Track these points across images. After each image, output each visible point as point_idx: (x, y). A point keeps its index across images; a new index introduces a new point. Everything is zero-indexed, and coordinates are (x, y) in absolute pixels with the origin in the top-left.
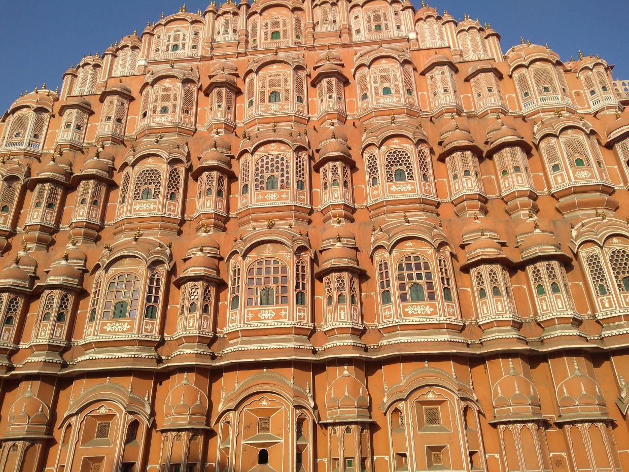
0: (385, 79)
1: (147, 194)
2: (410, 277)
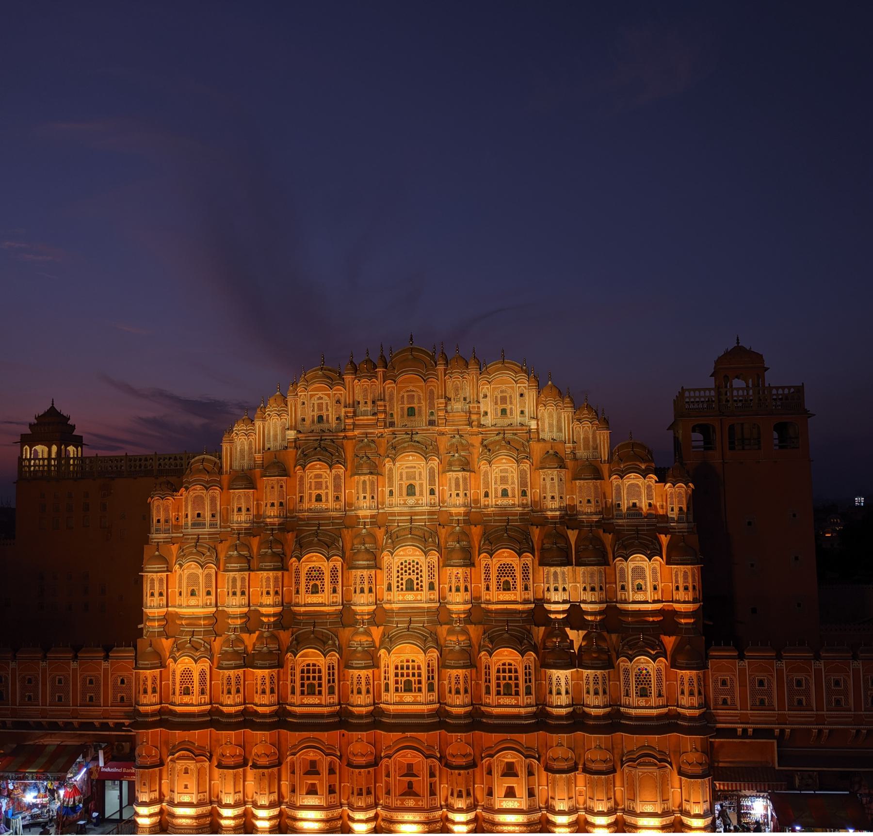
0: (504, 480)
1: (315, 590)
2: (504, 678)
